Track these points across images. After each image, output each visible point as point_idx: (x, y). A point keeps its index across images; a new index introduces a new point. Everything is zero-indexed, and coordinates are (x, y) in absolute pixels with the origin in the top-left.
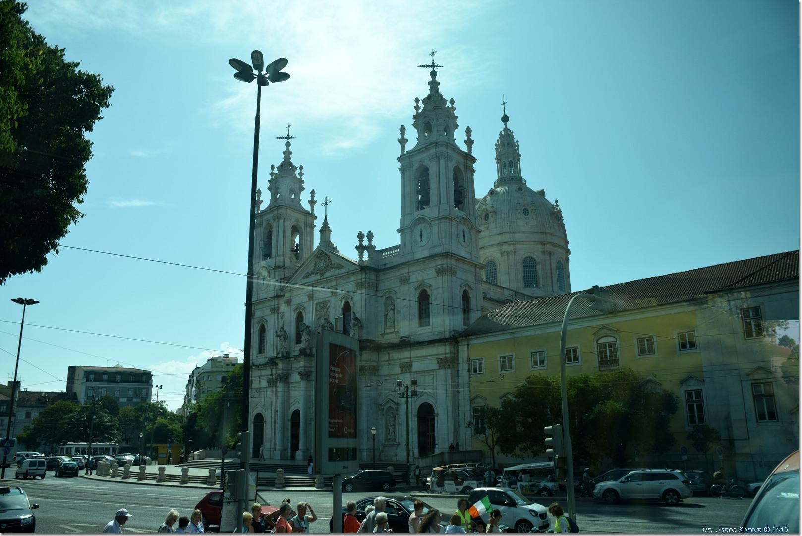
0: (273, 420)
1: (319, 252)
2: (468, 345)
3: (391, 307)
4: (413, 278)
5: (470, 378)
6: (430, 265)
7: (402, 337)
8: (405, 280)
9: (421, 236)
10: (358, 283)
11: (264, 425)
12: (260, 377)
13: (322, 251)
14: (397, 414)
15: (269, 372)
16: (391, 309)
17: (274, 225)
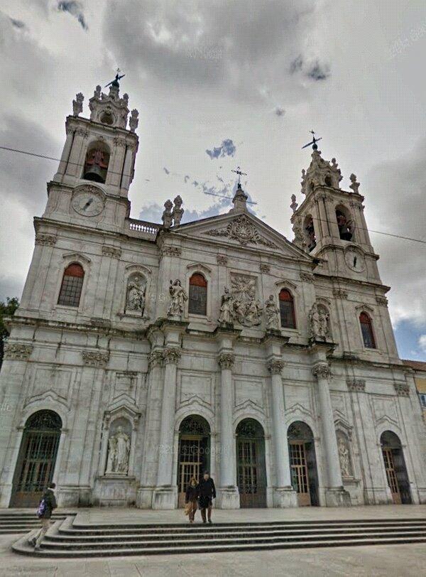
0: (92, 428)
1: (241, 216)
2: (414, 378)
3: (327, 316)
4: (351, 297)
5: (422, 411)
6: (369, 292)
7: (344, 352)
8: (340, 295)
9: (355, 262)
10: (305, 275)
11: (63, 436)
12: (60, 344)
13: (247, 217)
14: (351, 440)
15: (92, 342)
16: (327, 319)
17: (117, 153)
